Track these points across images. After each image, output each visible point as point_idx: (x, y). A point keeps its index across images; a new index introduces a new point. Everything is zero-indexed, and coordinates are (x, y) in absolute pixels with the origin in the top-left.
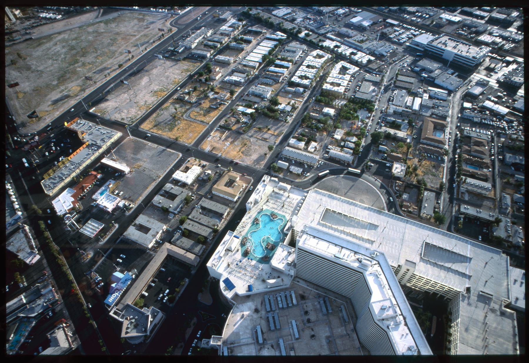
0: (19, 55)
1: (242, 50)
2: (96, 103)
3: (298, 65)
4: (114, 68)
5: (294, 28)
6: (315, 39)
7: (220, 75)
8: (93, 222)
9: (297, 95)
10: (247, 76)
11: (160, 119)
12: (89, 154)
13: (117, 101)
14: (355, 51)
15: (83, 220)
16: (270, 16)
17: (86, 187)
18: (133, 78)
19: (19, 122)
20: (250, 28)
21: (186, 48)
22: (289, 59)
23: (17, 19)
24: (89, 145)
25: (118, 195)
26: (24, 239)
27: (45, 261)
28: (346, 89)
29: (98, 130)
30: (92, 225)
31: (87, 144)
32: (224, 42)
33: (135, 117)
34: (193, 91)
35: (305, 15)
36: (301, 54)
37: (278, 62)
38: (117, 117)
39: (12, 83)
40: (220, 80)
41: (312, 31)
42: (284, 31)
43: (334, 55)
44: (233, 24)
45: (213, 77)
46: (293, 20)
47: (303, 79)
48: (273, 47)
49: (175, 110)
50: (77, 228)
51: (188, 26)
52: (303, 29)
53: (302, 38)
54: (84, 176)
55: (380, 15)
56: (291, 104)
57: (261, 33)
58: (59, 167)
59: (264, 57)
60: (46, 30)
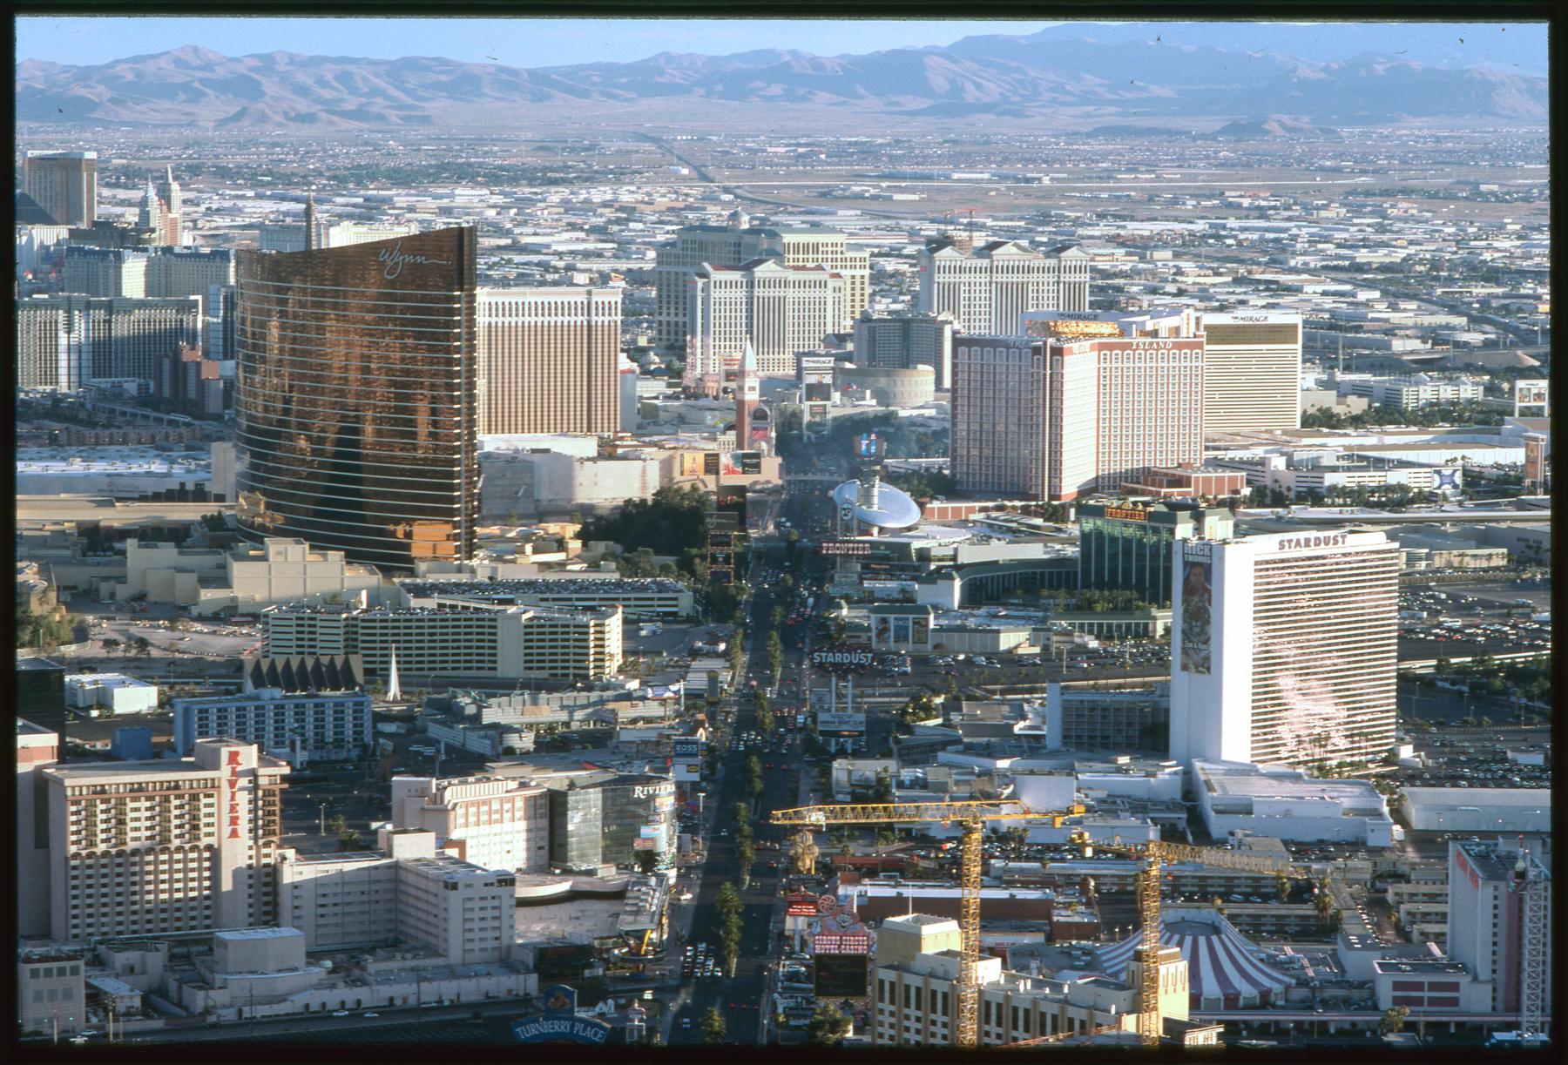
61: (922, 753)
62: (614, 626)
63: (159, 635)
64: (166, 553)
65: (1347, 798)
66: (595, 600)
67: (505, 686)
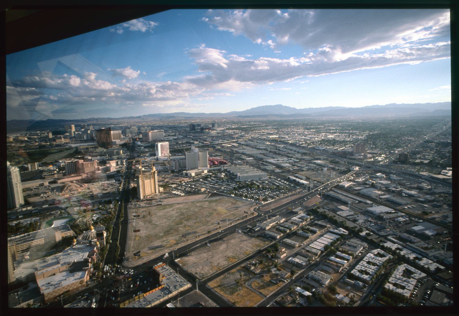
1: (307, 238)
2: (181, 256)
3: (358, 260)
4: (204, 233)
5: (356, 227)
6: (376, 239)
7: (285, 255)
9: (355, 288)
10: (309, 260)
11: (225, 282)
12: (160, 296)
13: (198, 257)
14: (420, 256)
16: (335, 215)
18: (215, 243)
19: (126, 256)
20: (316, 222)
21: (261, 228)
22: (350, 252)
23: (159, 192)
24: (164, 287)
28: (412, 294)
29: (175, 277)
31: (163, 286)
32: (292, 229)
33: (207, 274)
34: (259, 264)
35: (365, 218)
36: (362, 250)
37: (338, 253)
38: (192, 270)
40: (284, 259)
41: (372, 231)
42: (346, 228)
43: (397, 257)
44: (303, 216)
45: (278, 255)
46: (355, 221)
47: (363, 274)
48: (335, 239)
49: (240, 277)
51: (266, 213)
52: (364, 229)
53: (363, 237)
55: (444, 227)
56: (350, 296)
57: (326, 227)
58: (134, 300)
59: (326, 247)
61: (141, 157)
62: (121, 151)
63: (91, 154)
64: (92, 149)
65: (166, 158)
66: (120, 150)
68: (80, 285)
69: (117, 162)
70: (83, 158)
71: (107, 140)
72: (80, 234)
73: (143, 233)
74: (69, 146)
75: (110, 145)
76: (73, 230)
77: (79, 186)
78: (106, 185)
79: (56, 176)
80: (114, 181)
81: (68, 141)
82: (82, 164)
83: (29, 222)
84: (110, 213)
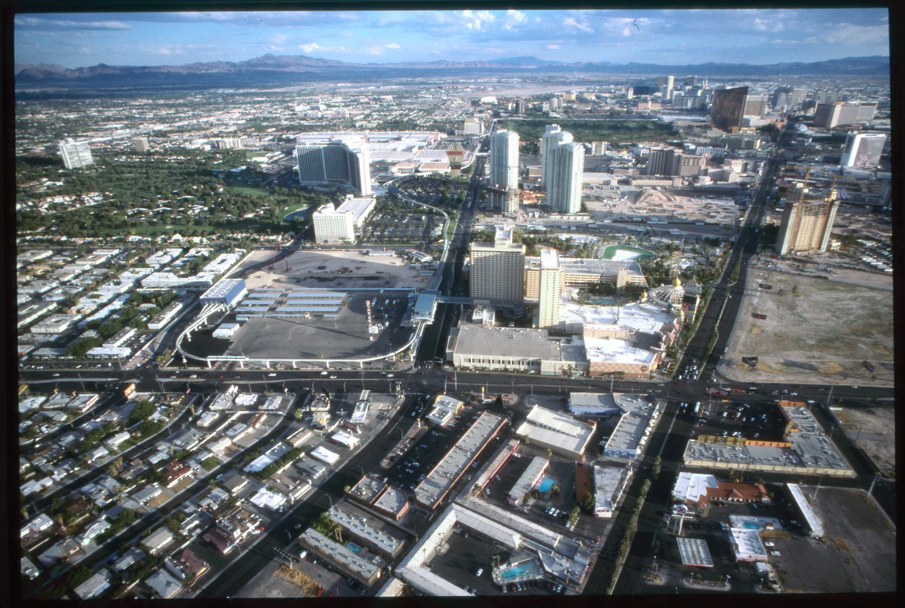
0: (794, 289)
2: (849, 404)
8: (704, 548)
12: (778, 460)
15: (695, 529)
17: (735, 495)
19: (727, 357)
24: (789, 448)
25: (769, 549)
26: (617, 482)
27: (610, 527)
29: (820, 441)
30: (698, 548)
31: (788, 445)
39: (759, 313)
50: (677, 532)
54: (745, 479)
60: (854, 277)
62: (759, 142)
63: (696, 139)
64: (699, 129)
67: (742, 149)
68: (640, 372)
69: (746, 165)
70: (680, 146)
71: (733, 113)
72: (654, 287)
73: (770, 325)
74: (659, 119)
75: (736, 125)
76: (645, 274)
77: (664, 198)
78: (714, 207)
79: (631, 171)
80: (733, 203)
81: (658, 107)
82: (679, 157)
83: (583, 242)
84: (712, 264)
